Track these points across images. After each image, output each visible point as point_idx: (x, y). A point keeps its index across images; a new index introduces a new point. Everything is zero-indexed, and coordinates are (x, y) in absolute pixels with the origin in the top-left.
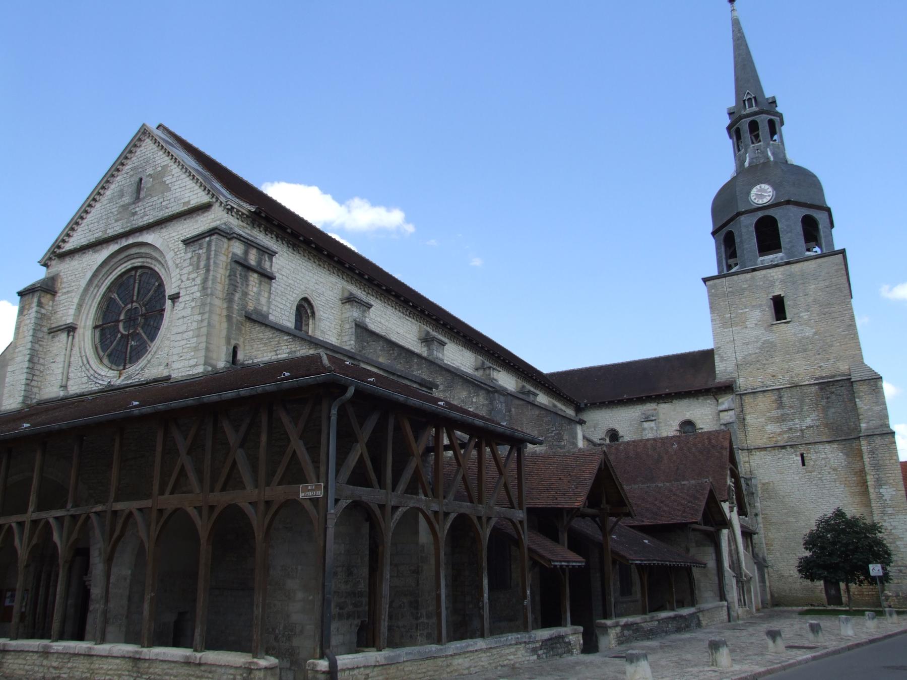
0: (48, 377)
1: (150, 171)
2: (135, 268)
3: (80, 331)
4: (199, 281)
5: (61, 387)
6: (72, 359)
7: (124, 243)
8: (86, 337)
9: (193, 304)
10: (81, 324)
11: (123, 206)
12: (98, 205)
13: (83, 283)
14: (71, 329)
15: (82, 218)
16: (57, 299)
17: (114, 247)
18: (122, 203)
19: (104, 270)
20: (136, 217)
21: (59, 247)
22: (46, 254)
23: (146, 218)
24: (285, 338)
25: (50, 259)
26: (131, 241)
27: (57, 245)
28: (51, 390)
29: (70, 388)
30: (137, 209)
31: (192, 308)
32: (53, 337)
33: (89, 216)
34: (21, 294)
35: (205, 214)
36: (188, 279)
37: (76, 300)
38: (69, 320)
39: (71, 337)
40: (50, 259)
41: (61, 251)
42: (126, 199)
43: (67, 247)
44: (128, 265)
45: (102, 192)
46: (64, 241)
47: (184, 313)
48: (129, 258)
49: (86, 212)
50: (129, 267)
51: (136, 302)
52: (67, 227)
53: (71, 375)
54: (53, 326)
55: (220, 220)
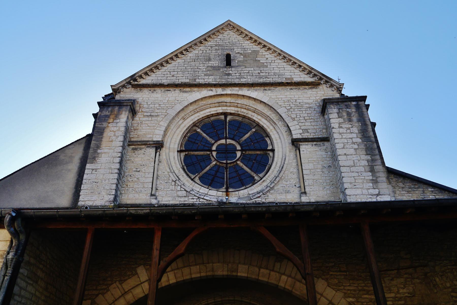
0: (130, 184)
1: (237, 50)
2: (225, 114)
3: (164, 151)
4: (355, 130)
5: (152, 195)
6: (160, 172)
7: (220, 91)
8: (172, 156)
9: (356, 147)
10: (166, 144)
11: (211, 67)
12: (179, 60)
13: (172, 113)
14: (158, 146)
15: (162, 65)
16: (137, 118)
17: (205, 92)
18: (210, 65)
19: (191, 108)
20: (230, 77)
21: (135, 80)
22: (122, 82)
23: (241, 80)
24: (430, 190)
25: (124, 86)
26: (228, 91)
27: (133, 78)
28: (137, 195)
29: (159, 198)
30: (231, 72)
31: (356, 149)
32: (136, 149)
33: (169, 65)
34: (99, 103)
35: (314, 90)
36: (340, 127)
37: (164, 124)
38: (158, 138)
39: (158, 154)
40: (124, 86)
41: (136, 83)
42: (215, 63)
43: (142, 82)
44: (220, 110)
45: (184, 53)
46: (141, 77)
47: (344, 151)
48: (220, 104)
49: (167, 62)
50: (221, 111)
51: (229, 138)
52: (147, 67)
53: (160, 187)
54: (132, 140)
55: (332, 96)
